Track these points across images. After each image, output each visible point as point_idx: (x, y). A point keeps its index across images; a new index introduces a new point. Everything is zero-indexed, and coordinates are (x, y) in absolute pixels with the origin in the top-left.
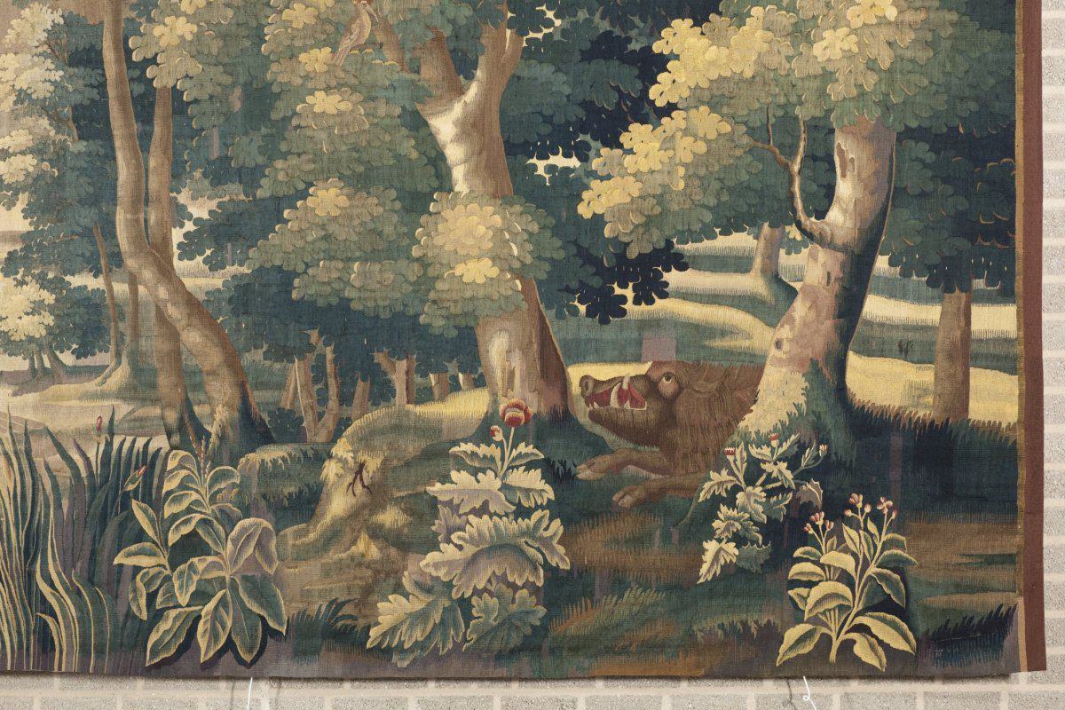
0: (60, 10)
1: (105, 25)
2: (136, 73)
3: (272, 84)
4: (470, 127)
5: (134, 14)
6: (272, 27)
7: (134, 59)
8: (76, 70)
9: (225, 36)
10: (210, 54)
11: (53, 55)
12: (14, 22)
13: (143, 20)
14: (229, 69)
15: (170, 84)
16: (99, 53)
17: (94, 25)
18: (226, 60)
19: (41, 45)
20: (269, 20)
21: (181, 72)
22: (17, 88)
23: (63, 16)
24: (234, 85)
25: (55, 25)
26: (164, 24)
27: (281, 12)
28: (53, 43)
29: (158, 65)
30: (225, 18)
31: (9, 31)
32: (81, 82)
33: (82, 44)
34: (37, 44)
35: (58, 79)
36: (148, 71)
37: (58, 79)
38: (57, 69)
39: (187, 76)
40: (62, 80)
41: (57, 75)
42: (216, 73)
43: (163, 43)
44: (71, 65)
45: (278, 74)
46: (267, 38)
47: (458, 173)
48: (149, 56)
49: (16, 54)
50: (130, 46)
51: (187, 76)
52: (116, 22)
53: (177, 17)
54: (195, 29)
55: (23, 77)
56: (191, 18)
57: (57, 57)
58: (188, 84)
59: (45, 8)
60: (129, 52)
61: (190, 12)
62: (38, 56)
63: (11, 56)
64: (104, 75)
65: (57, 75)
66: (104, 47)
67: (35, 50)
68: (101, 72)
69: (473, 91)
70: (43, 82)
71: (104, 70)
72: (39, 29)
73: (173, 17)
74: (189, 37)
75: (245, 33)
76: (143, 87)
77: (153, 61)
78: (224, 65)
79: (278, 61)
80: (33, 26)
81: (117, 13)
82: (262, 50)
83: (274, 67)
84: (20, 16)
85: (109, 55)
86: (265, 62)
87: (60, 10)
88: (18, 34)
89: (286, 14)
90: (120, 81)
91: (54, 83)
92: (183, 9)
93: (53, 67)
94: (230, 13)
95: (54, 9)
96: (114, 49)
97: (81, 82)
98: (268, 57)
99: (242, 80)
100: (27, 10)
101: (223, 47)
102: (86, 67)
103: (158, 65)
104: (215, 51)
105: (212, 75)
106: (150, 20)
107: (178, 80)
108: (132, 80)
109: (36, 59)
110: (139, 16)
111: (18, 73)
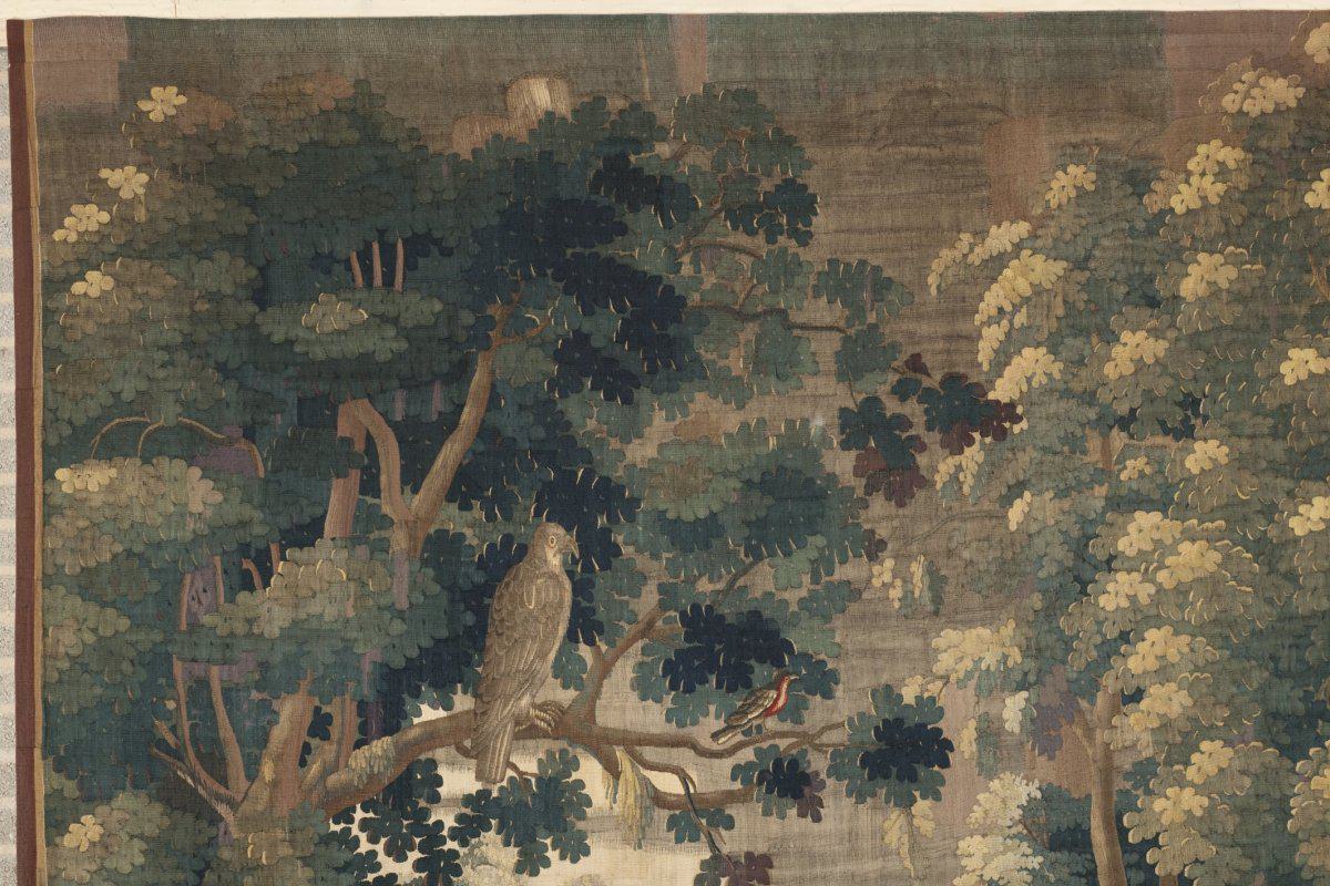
0: (1036, 781)
1: (1094, 798)
2: (1134, 858)
3: (1301, 869)
5: (1128, 785)
6: (1299, 799)
7: (1131, 840)
8: (1059, 855)
9: (1242, 811)
10: (1225, 833)
11: (1030, 837)
12: (981, 797)
13: (1140, 792)
14: (1250, 851)
15: (1176, 873)
16: (1087, 833)
17: (1079, 800)
18: (1245, 840)
19: (1016, 824)
20: (1296, 790)
21: (1190, 855)
22: (987, 878)
23: (1040, 789)
24: (1256, 869)
25: (1031, 800)
26: (1166, 797)
27: (1309, 779)
28: (1029, 822)
29: (1160, 847)
30: (1241, 788)
31: (975, 808)
32: (1066, 870)
33: (1066, 822)
34: (1010, 823)
35: (1037, 867)
36: (1148, 855)
37: (1037, 867)
38: (1034, 854)
39: (1197, 861)
40: (1042, 868)
41: (1035, 862)
42: (1233, 856)
43: (1165, 820)
44: (1051, 849)
46: (1293, 812)
48: (1149, 836)
49: (984, 836)
50: (1125, 824)
51: (1197, 861)
52: (1107, 794)
53: (1182, 788)
54: (1206, 802)
55: (993, 864)
56: (1199, 789)
57: (1034, 839)
58: (1199, 870)
59: (1018, 779)
60: (1123, 832)
61: (1198, 780)
62: (1011, 838)
63: (978, 838)
64: (1093, 861)
65: (1035, 862)
66: (1093, 827)
67: (1007, 831)
68: (1089, 856)
70: (1018, 871)
71: (1093, 855)
72: (1013, 805)
73: (1177, 788)
74: (1199, 813)
75: (1268, 806)
76: (1142, 874)
77: (1153, 843)
78: (1243, 846)
79: (1308, 841)
80: (1004, 801)
81: (1107, 783)
82: (1289, 826)
83: (1304, 848)
84: (987, 789)
85: (1098, 836)
86: (1293, 842)
87: (1036, 781)
88: (986, 812)
89: (1315, 783)
90: (1113, 868)
91: (1031, 871)
92: (1189, 778)
93: (1029, 851)
94: (1247, 782)
95: (1029, 779)
96: (1105, 828)
97: (1066, 870)
98: (1295, 835)
99: (1264, 863)
100: (996, 781)
101: (1240, 824)
102: (1070, 851)
103: (1160, 847)
104: (1230, 829)
105: (1227, 859)
106: (1149, 792)
107: (1185, 866)
108: (1129, 866)
109: (1009, 842)
110: (1135, 787)
111: (987, 859)
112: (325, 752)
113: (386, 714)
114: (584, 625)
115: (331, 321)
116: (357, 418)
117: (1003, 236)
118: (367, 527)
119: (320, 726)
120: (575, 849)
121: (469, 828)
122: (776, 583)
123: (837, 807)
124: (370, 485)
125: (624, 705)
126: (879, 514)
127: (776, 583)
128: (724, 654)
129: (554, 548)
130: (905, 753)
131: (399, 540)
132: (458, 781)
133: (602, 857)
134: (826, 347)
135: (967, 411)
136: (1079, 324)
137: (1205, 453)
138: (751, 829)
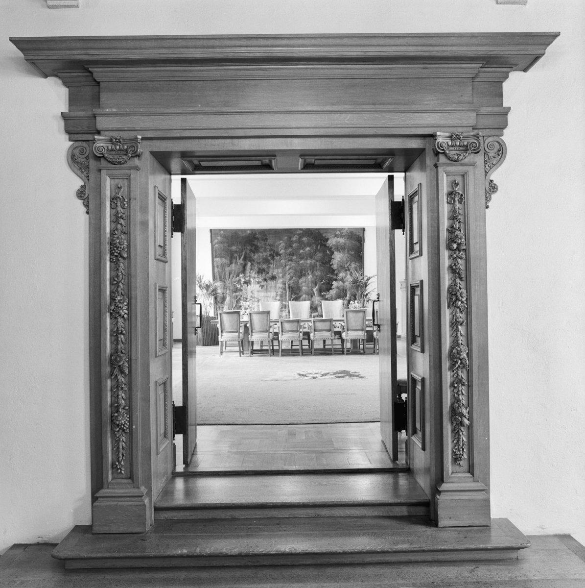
4: (316, 290)
45: (300, 286)
47: (315, 294)
69: (317, 287)
112: (234, 278)
113: (238, 276)
114: (251, 269)
115: (234, 248)
116: (236, 255)
117: (281, 242)
118: (236, 263)
119: (233, 277)
120: (251, 285)
121: (243, 283)
122: (265, 266)
123: (269, 282)
124: (237, 260)
125: (253, 274)
126: (272, 261)
127: (265, 266)
128: (261, 271)
129: (249, 264)
130: (273, 278)
131: (239, 263)
132: (243, 280)
133: (252, 285)
134: (268, 250)
135: (278, 254)
136: (286, 248)
137: (294, 257)
138: (263, 283)
